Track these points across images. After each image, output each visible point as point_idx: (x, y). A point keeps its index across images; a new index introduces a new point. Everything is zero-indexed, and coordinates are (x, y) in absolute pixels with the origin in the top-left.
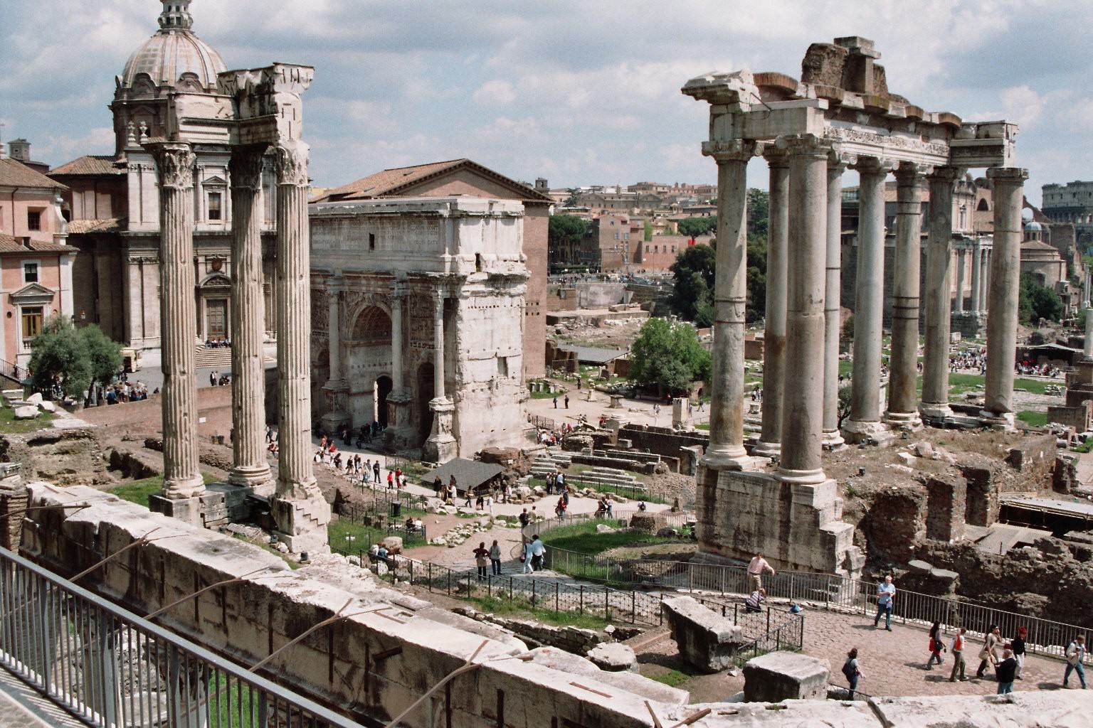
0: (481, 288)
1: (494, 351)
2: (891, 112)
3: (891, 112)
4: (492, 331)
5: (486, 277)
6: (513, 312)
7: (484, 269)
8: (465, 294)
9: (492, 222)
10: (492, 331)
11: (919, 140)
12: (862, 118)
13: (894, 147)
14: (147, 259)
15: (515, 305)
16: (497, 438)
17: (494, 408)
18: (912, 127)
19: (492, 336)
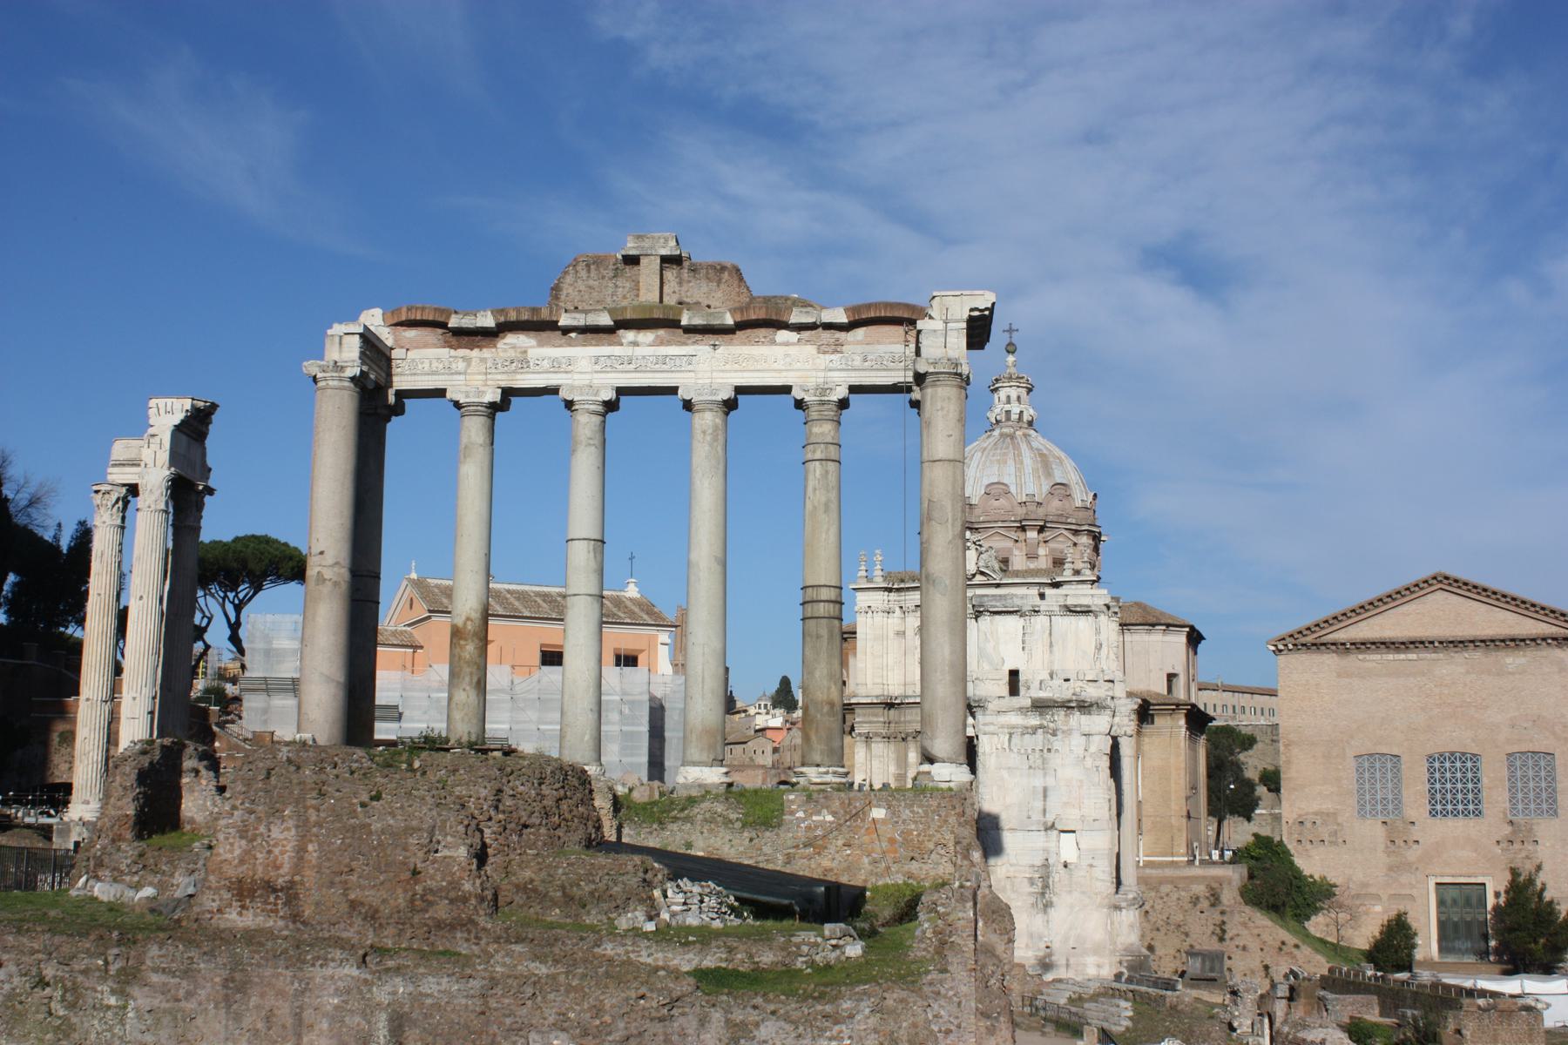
0: (1016, 719)
1: (1050, 818)
2: (684, 322)
3: (684, 322)
4: (1045, 790)
5: (1028, 703)
6: (1089, 762)
7: (1022, 690)
8: (987, 729)
9: (1040, 622)
10: (1045, 790)
11: (811, 349)
12: (629, 335)
13: (728, 367)
14: (877, 734)
15: (1093, 749)
16: (1059, 959)
17: (1052, 911)
18: (783, 335)
19: (1045, 796)
